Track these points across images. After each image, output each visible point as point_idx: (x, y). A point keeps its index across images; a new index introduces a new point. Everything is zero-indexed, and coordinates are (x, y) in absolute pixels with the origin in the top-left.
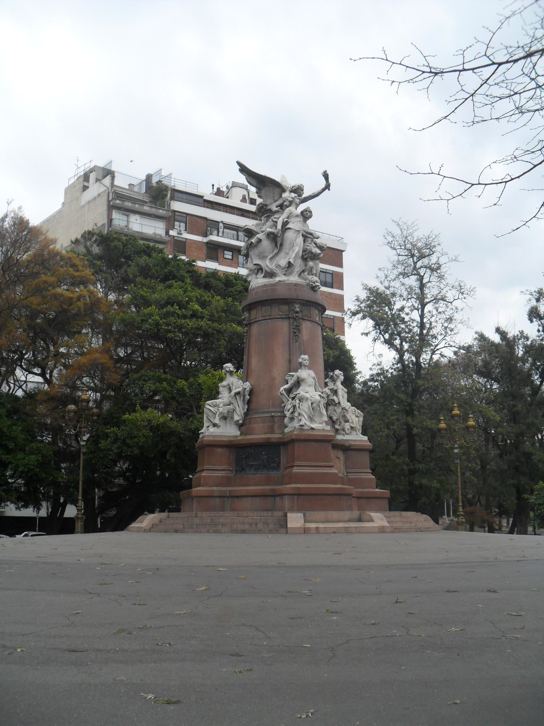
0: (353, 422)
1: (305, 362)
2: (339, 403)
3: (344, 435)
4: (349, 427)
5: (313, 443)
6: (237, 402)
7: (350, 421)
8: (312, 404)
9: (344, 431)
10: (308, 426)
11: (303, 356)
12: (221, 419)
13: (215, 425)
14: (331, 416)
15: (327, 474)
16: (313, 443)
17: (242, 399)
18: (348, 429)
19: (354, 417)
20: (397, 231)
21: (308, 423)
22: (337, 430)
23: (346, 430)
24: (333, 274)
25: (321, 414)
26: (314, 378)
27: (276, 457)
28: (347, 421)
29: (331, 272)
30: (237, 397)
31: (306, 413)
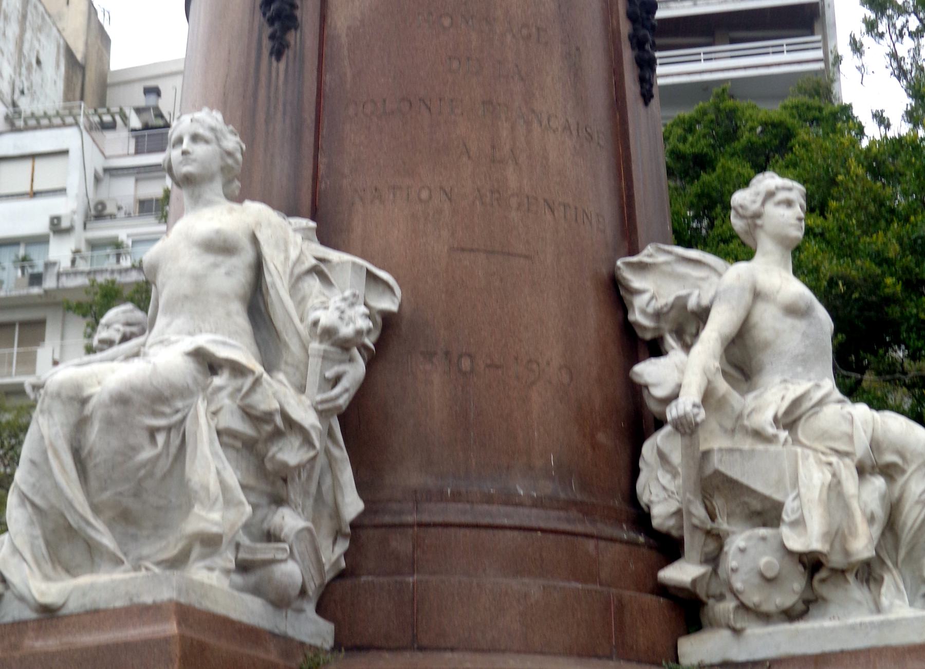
10: (21, 599)
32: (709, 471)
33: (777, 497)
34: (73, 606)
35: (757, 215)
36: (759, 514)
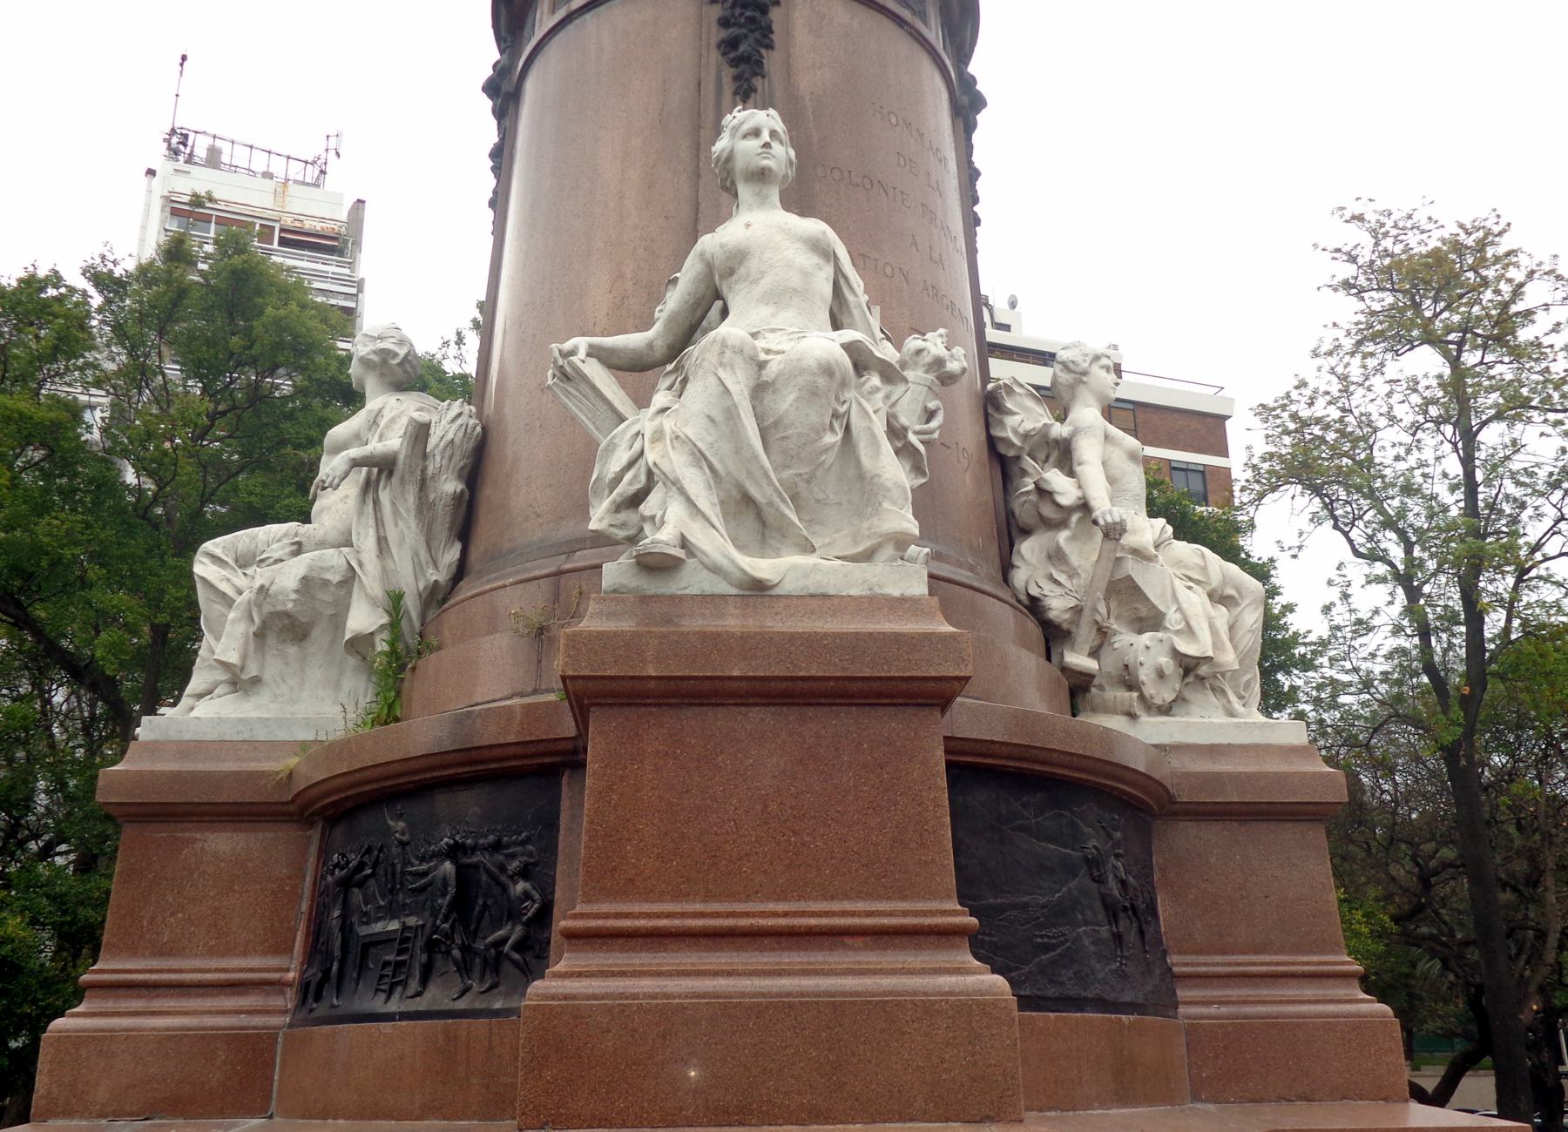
0: (1189, 631)
1: (753, 144)
2: (1084, 506)
3: (1132, 716)
4: (1165, 661)
5: (758, 718)
6: (379, 523)
7: (1172, 618)
8: (760, 390)
9: (1131, 684)
10: (716, 570)
11: (741, 117)
12: (271, 640)
13: (239, 682)
14: (1034, 591)
15: (884, 1008)
16: (756, 713)
17: (411, 498)
18: (1161, 675)
19: (1195, 602)
20: (1359, 238)
21: (715, 543)
22: (1078, 688)
23: (1145, 675)
24: (1203, 472)
25: (865, 490)
26: (829, 255)
27: (524, 873)
28: (1149, 620)
29: (1201, 468)
30: (385, 496)
31: (699, 457)
32: (1120, 575)
33: (1162, 608)
34: (789, 587)
35: (1085, 373)
36: (1140, 620)
